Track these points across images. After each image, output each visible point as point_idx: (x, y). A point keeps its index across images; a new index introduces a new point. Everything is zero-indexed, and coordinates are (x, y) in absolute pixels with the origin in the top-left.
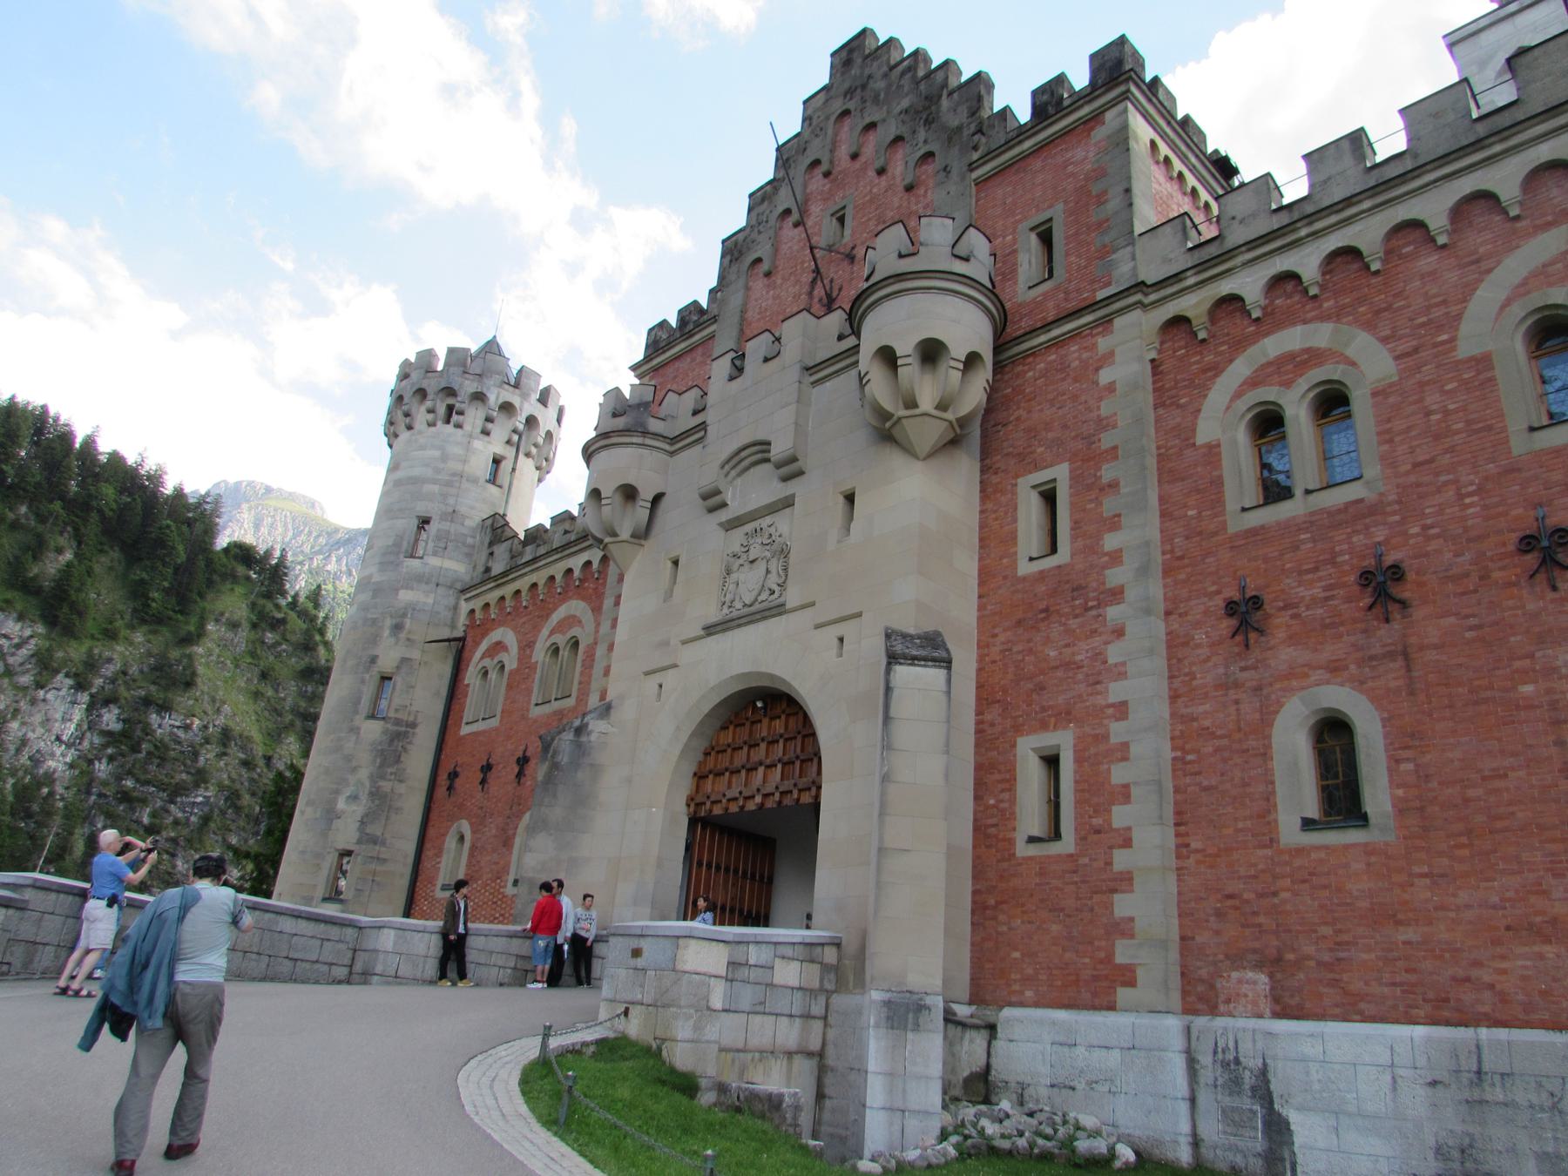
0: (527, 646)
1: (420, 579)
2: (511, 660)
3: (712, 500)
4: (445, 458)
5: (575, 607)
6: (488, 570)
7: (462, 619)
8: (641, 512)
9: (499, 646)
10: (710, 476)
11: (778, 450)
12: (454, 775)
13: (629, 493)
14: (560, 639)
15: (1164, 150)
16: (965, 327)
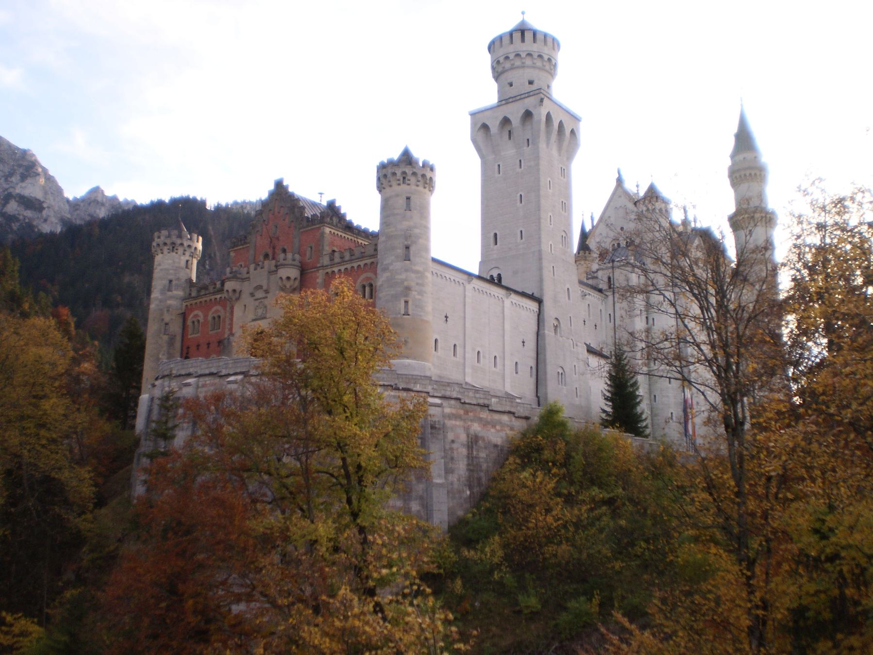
0: (206, 316)
1: (171, 298)
2: (201, 319)
3: (252, 295)
4: (174, 262)
5: (219, 308)
6: (190, 294)
7: (184, 307)
8: (237, 295)
9: (196, 316)
10: (251, 290)
11: (265, 287)
12: (188, 348)
13: (234, 291)
14: (215, 315)
15: (333, 231)
16: (294, 273)
